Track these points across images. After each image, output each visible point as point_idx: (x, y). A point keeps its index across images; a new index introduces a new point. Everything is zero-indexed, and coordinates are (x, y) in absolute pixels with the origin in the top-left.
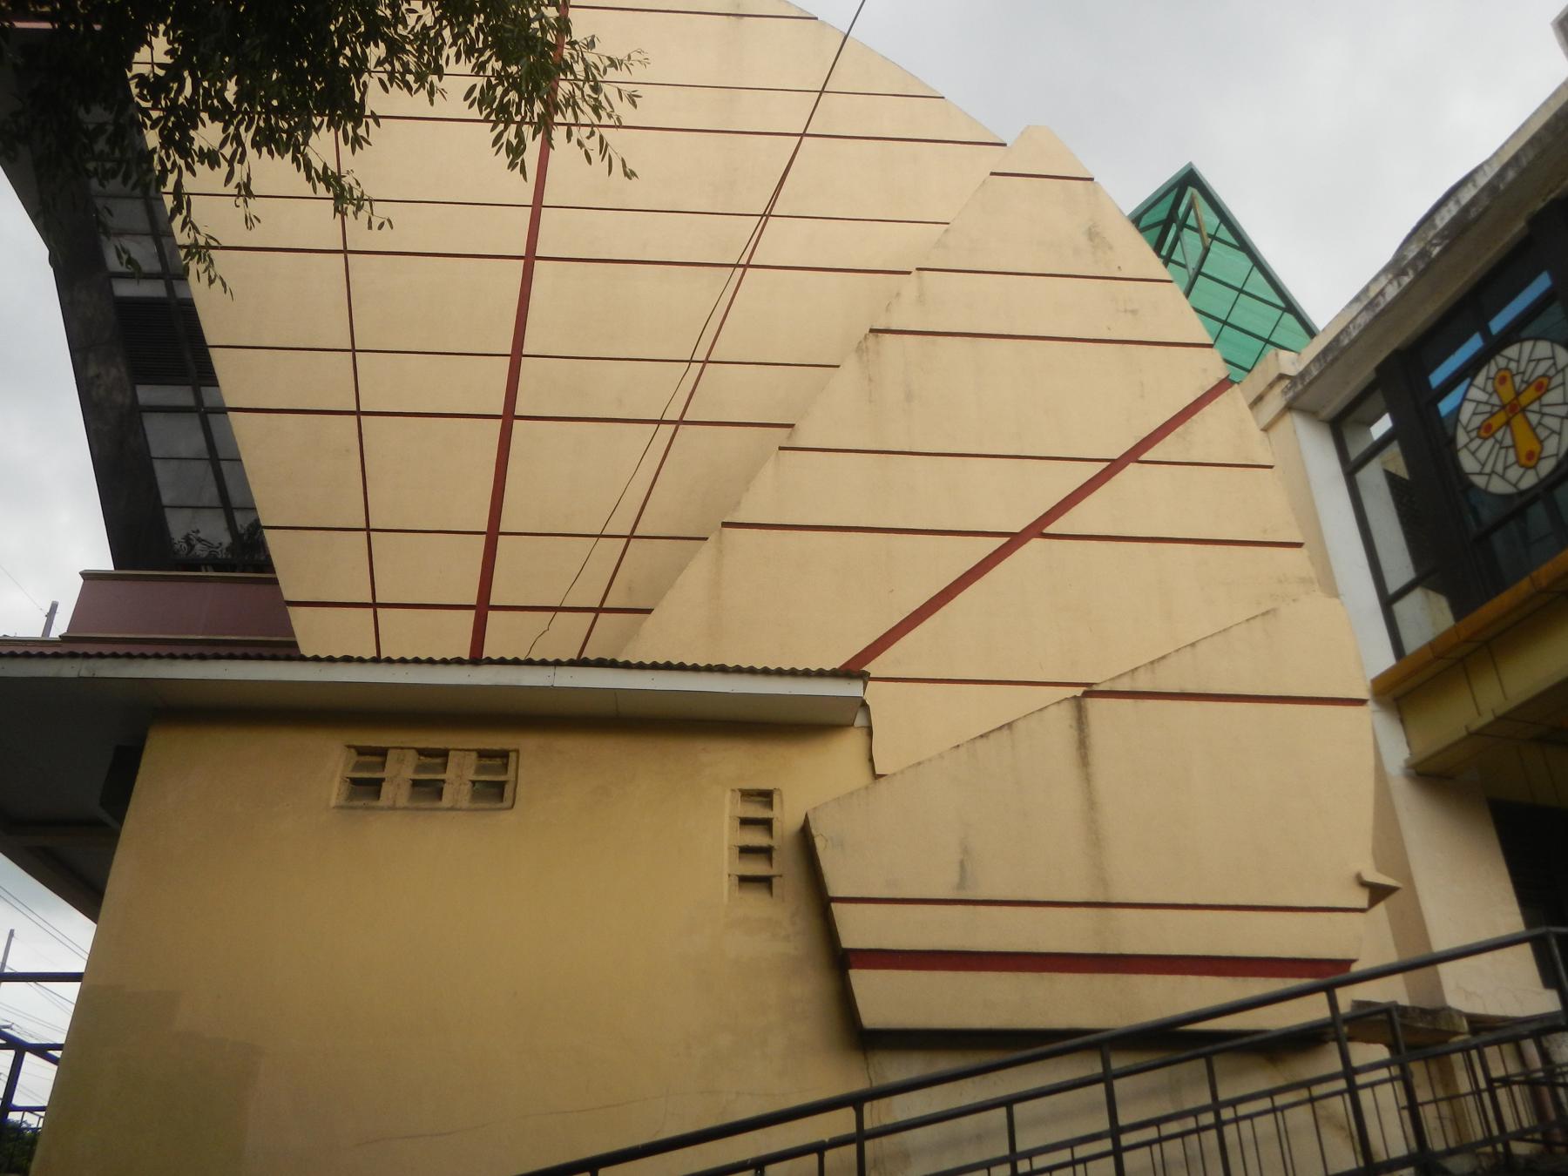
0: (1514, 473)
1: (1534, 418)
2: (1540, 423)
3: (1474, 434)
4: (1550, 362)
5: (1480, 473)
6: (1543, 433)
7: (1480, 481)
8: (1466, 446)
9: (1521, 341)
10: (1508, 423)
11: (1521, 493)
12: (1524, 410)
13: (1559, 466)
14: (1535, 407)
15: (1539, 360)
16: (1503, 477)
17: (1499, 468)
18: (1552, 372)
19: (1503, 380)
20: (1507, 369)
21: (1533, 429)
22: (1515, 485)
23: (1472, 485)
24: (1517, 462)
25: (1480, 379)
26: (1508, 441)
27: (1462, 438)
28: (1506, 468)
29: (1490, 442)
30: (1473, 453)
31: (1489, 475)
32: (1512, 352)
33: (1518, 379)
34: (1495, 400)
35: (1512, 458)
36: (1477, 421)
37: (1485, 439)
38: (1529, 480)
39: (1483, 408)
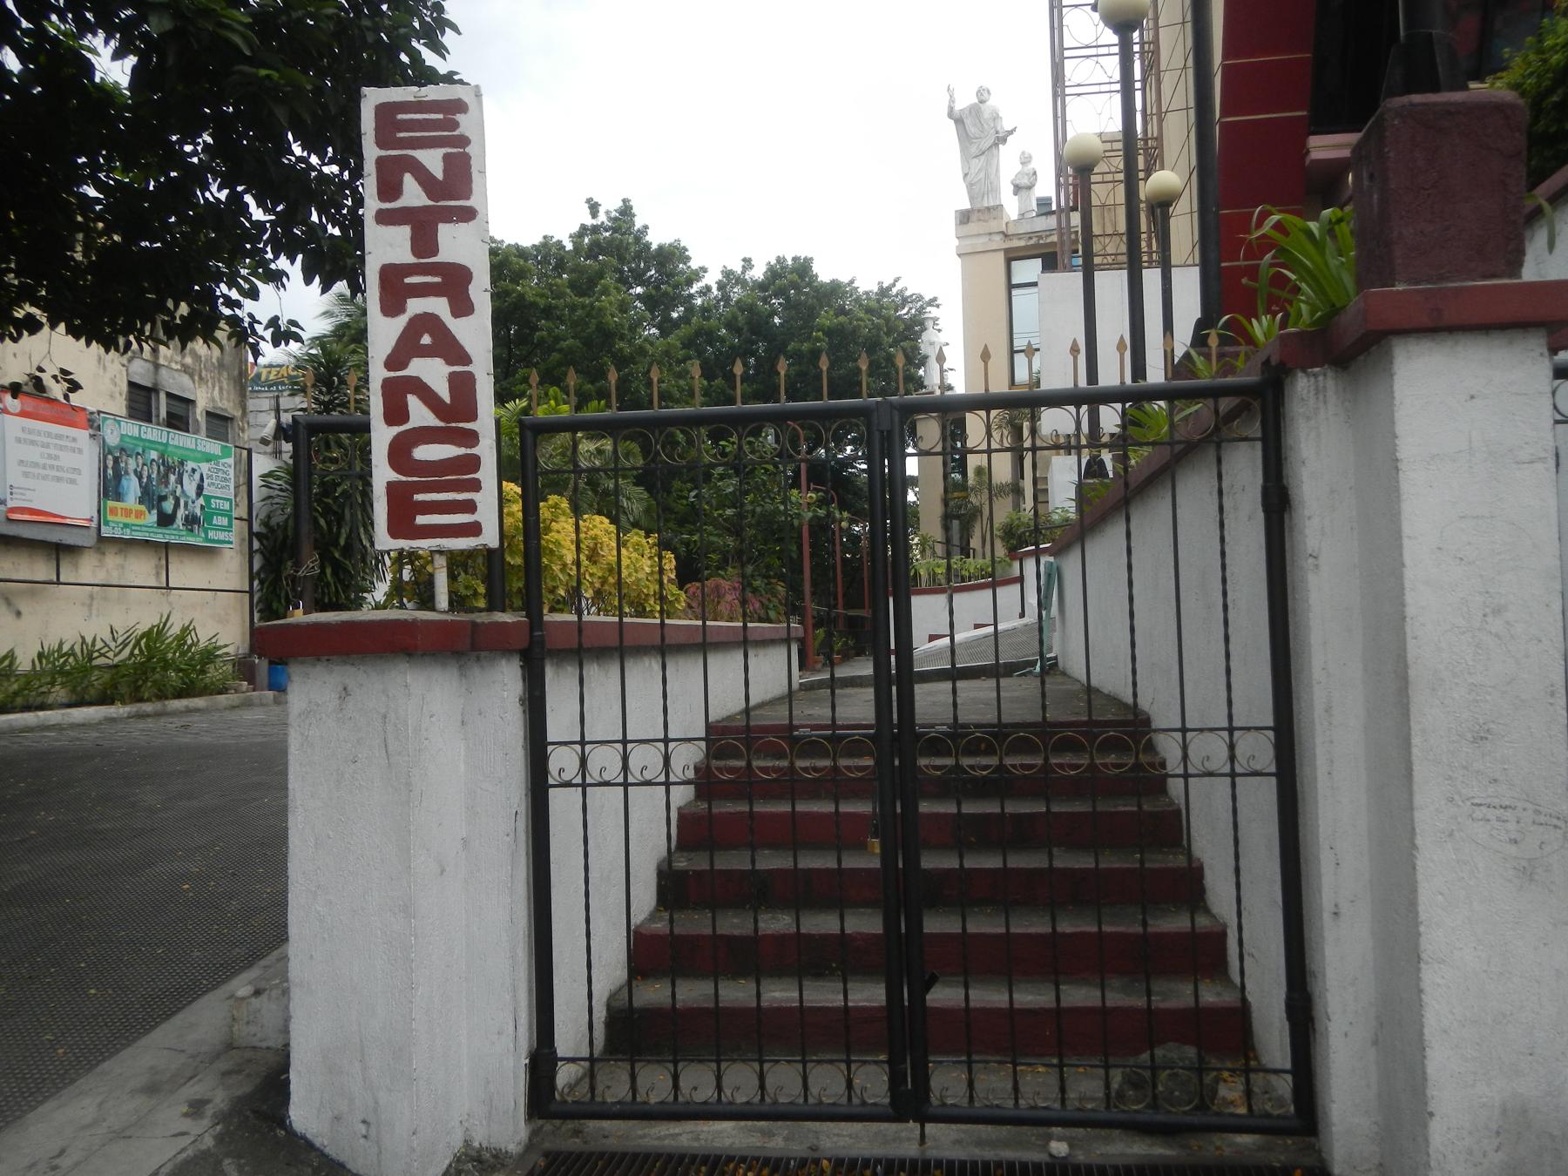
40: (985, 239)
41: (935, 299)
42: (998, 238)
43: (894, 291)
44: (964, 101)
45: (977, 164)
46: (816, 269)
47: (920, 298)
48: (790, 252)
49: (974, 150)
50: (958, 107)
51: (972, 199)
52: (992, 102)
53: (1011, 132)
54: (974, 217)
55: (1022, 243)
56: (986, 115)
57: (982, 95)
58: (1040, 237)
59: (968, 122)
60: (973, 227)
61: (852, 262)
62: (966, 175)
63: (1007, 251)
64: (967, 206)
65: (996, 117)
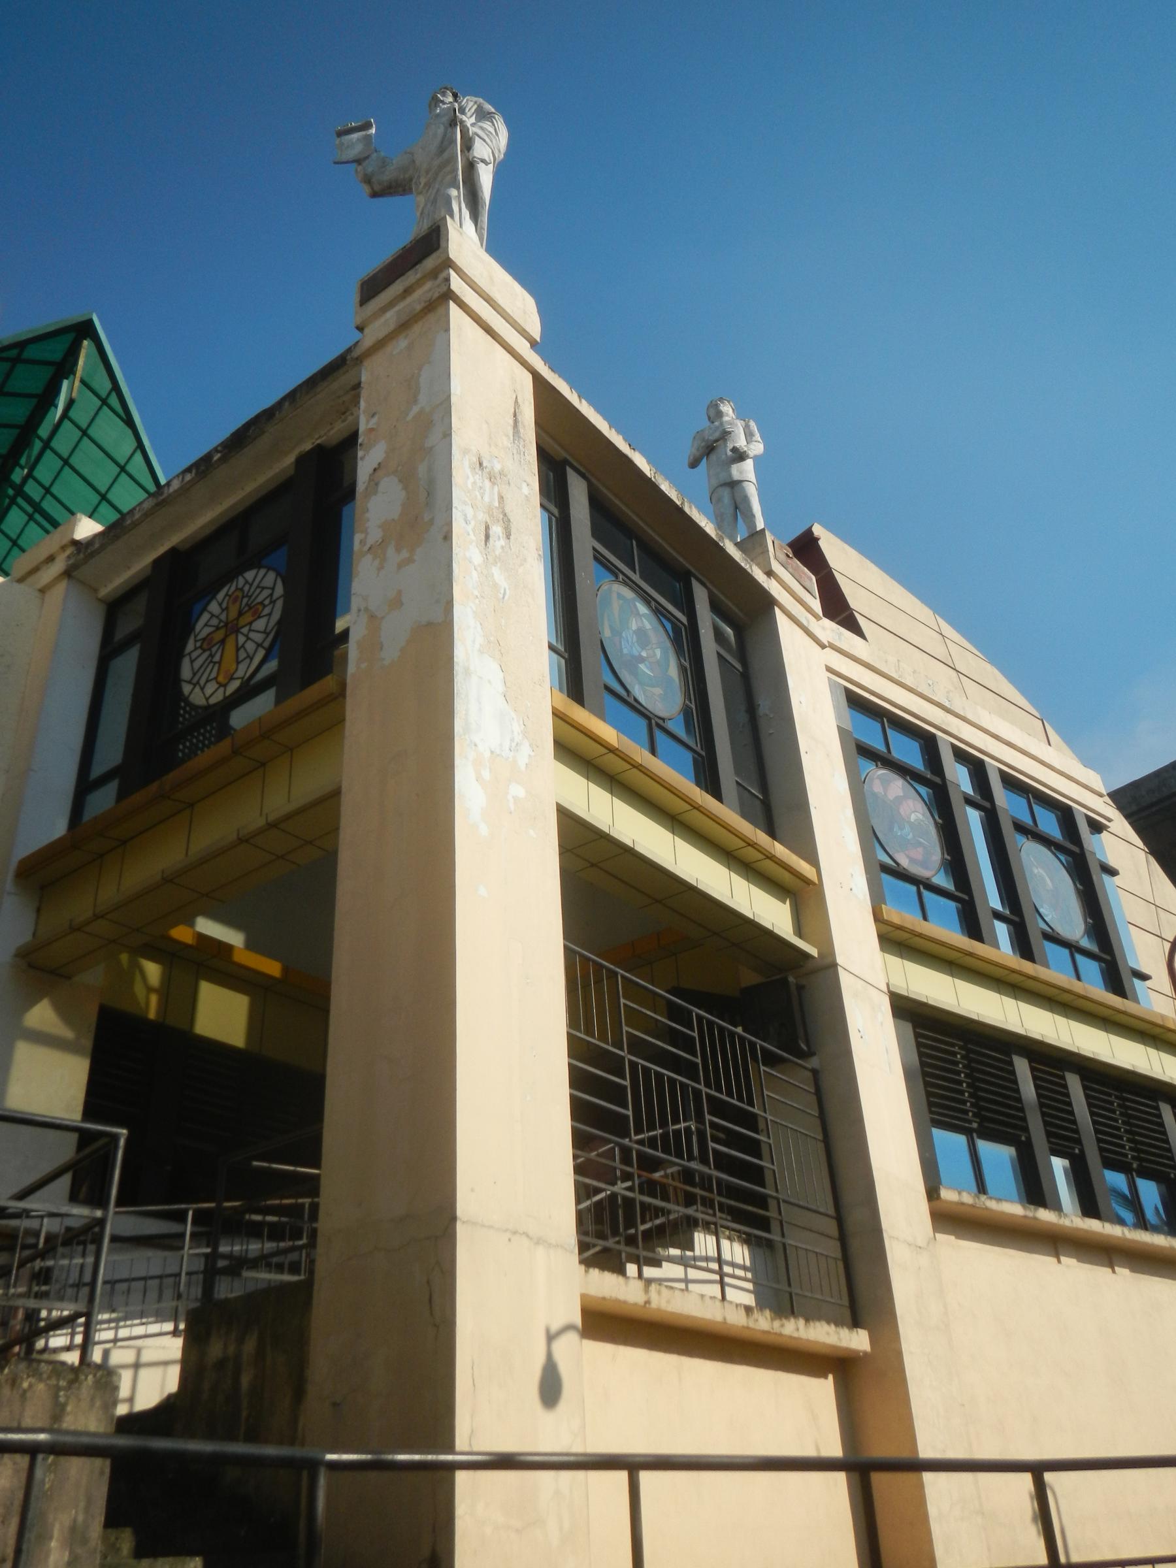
2: (243, 646)
3: (198, 644)
4: (269, 591)
5: (189, 682)
7: (186, 688)
8: (189, 654)
9: (259, 567)
11: (208, 707)
15: (263, 588)
16: (202, 689)
17: (202, 682)
18: (267, 602)
20: (242, 590)
21: (238, 650)
22: (207, 699)
23: (180, 692)
27: (190, 646)
28: (207, 681)
29: (207, 653)
30: (192, 662)
31: (195, 685)
33: (245, 600)
34: (223, 617)
37: (204, 651)
38: (218, 697)
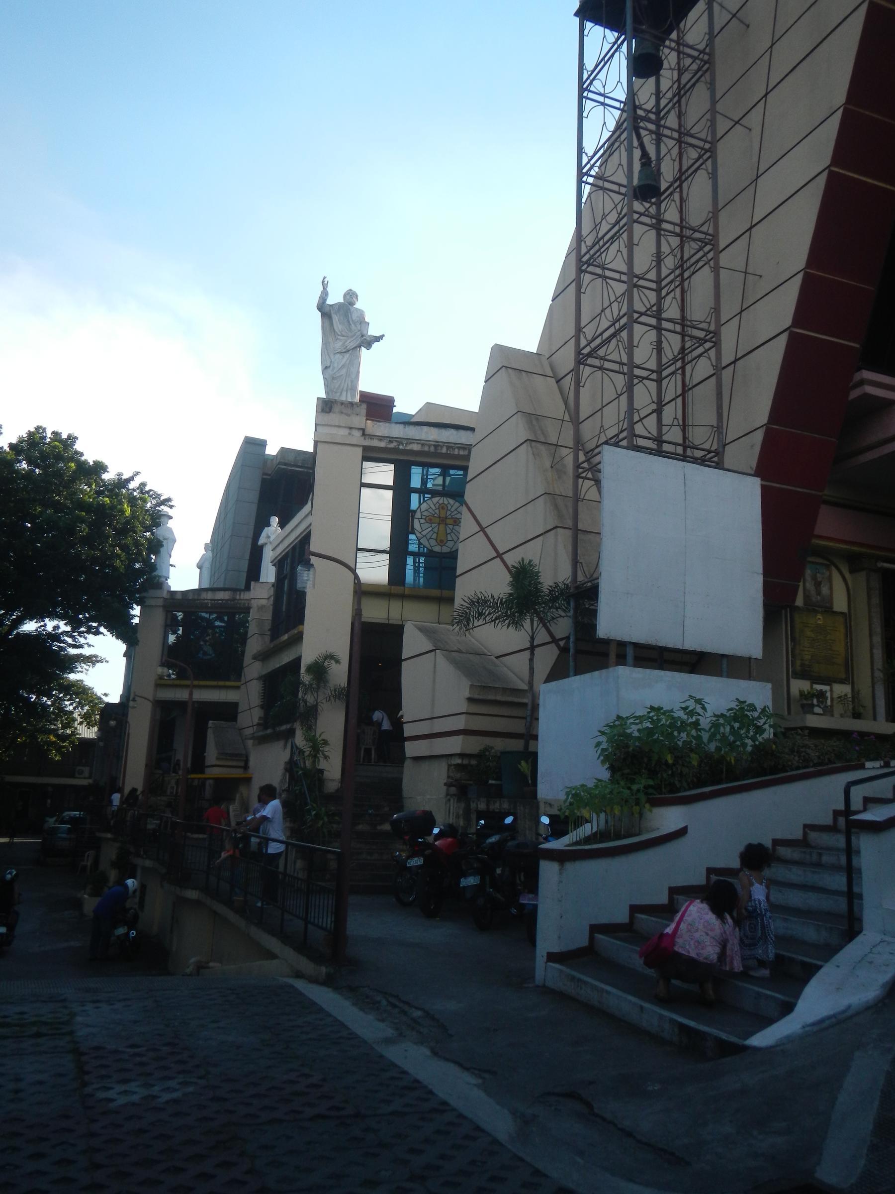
0: (433, 542)
1: (449, 531)
6: (449, 538)
10: (439, 524)
12: (446, 524)
13: (450, 552)
14: (451, 527)
19: (443, 508)
24: (436, 540)
25: (436, 500)
26: (436, 530)
32: (451, 501)
35: (434, 536)
36: (425, 513)
38: (437, 549)
39: (430, 510)
40: (346, 431)
41: (169, 500)
42: (358, 434)
43: (132, 485)
44: (336, 297)
45: (340, 360)
46: (78, 447)
47: (158, 496)
48: (56, 423)
49: (338, 345)
50: (330, 301)
51: (327, 393)
52: (358, 305)
53: (378, 339)
54: (337, 408)
55: (382, 444)
56: (355, 317)
57: (351, 297)
58: (400, 443)
59: (335, 318)
60: (334, 418)
61: (114, 447)
62: (325, 369)
63: (365, 449)
64: (323, 395)
65: (362, 322)
